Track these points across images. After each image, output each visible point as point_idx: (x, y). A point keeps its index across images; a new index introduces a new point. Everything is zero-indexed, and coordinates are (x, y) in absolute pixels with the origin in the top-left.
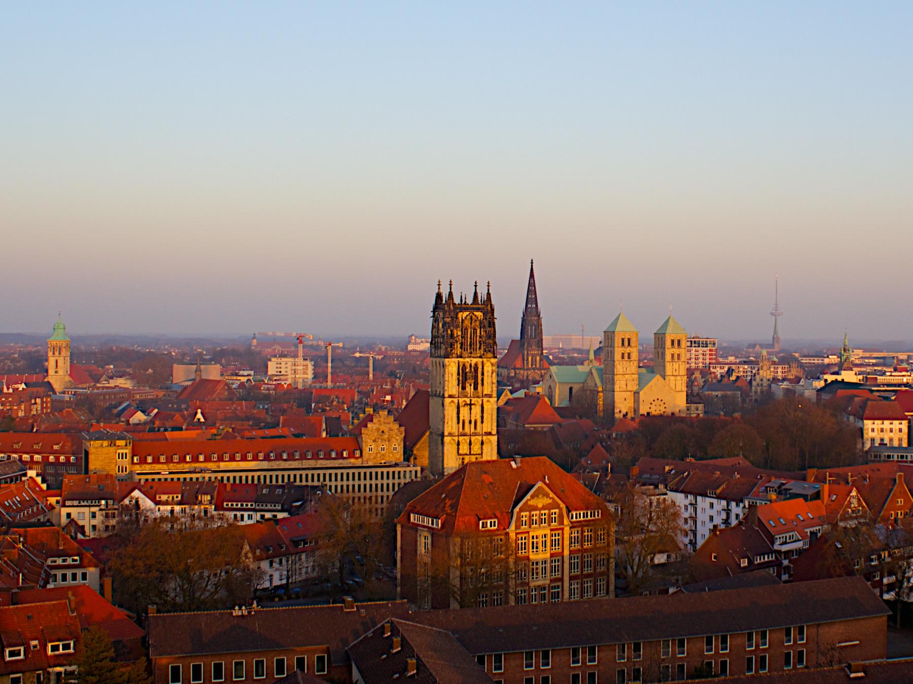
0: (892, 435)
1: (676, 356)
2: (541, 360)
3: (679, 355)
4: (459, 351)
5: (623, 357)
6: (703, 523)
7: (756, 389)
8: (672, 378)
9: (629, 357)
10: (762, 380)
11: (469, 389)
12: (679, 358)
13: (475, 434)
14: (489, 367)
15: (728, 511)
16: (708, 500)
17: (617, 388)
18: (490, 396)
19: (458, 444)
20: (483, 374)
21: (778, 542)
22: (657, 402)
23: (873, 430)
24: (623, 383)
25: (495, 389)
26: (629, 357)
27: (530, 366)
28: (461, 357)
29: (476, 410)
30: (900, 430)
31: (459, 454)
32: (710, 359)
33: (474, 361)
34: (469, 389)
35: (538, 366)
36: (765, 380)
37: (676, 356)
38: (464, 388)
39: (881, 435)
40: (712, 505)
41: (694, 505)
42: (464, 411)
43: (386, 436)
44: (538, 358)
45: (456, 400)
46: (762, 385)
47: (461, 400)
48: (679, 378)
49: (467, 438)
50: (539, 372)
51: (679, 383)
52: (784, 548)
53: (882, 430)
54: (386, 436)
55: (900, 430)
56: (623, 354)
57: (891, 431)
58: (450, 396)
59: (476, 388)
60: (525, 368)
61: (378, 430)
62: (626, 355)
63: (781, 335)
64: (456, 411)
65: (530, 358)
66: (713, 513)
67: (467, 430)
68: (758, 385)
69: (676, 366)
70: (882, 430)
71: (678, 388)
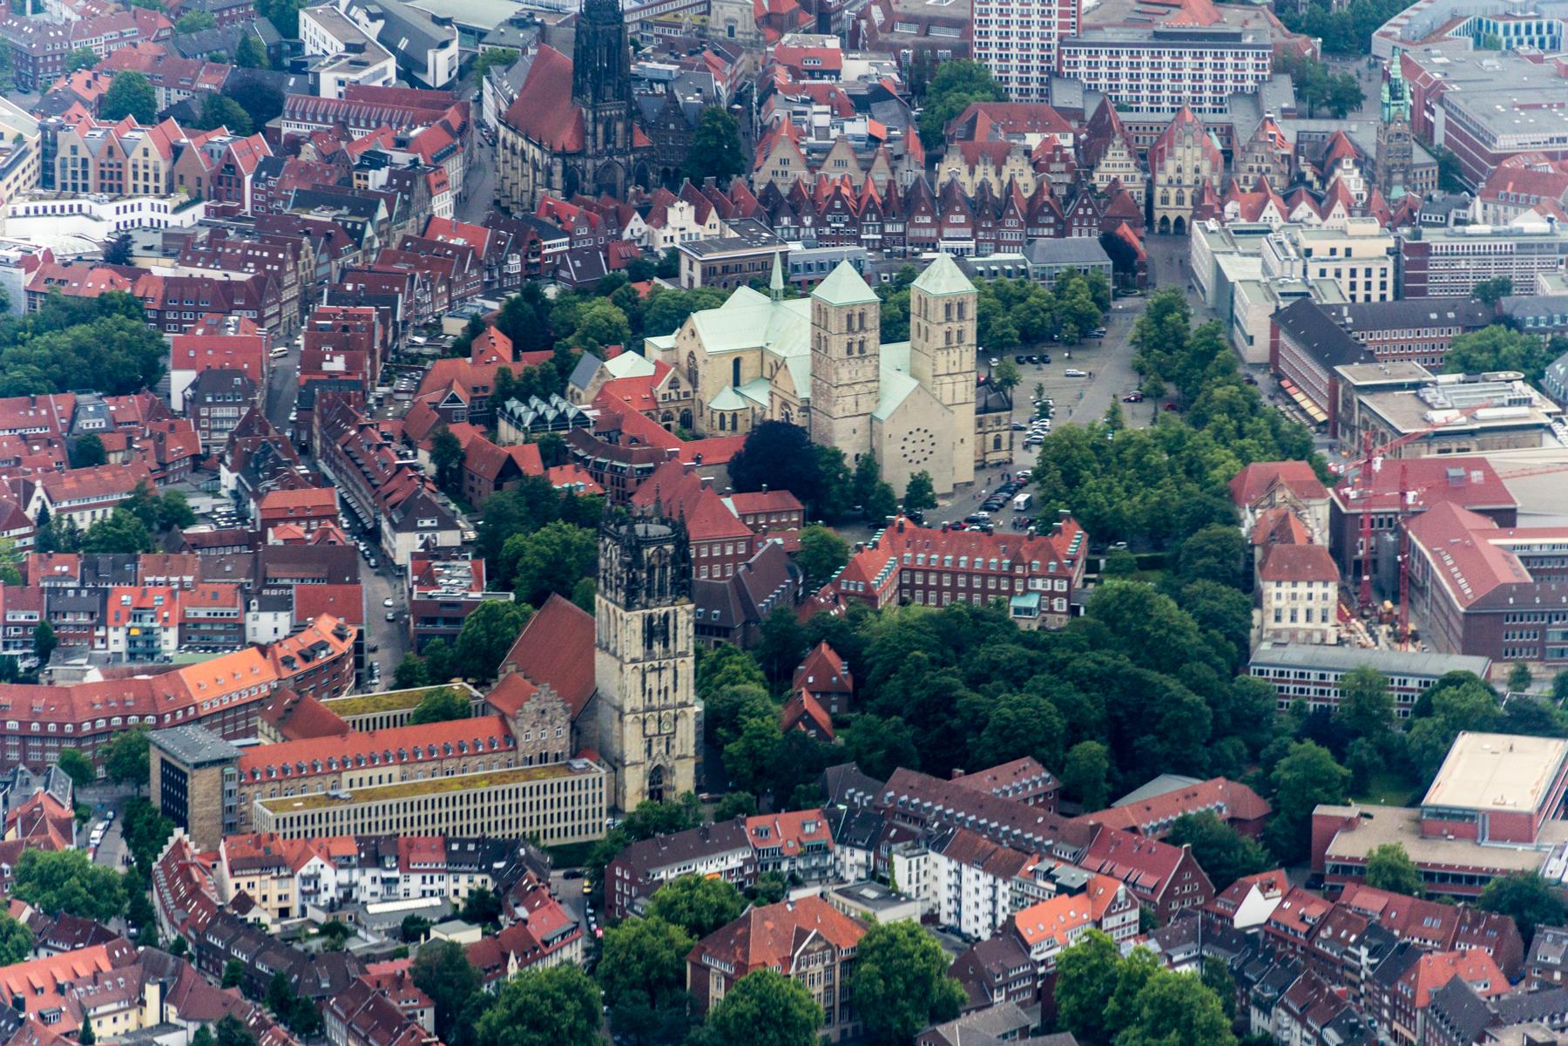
0: (1310, 604)
1: (954, 336)
2: (629, 130)
3: (960, 333)
4: (644, 600)
5: (849, 351)
6: (969, 894)
7: (1165, 190)
8: (947, 379)
9: (861, 350)
10: (1179, 170)
11: (658, 648)
12: (960, 340)
13: (666, 707)
14: (683, 615)
15: (995, 888)
16: (974, 871)
17: (837, 411)
18: (685, 654)
19: (644, 722)
20: (676, 627)
21: (1033, 952)
22: (917, 436)
23: (1279, 596)
24: (850, 400)
25: (692, 645)
26: (861, 350)
27: (600, 147)
28: (646, 607)
29: (668, 675)
30: (1325, 597)
31: (645, 735)
32: (1062, 26)
33: (664, 610)
34: (658, 648)
35: (619, 145)
36: (1188, 171)
37: (954, 336)
38: (650, 647)
39: (1293, 604)
40: (978, 877)
41: (959, 873)
42: (652, 679)
43: (547, 718)
44: (620, 127)
45: (640, 665)
46: (1179, 181)
47: (647, 664)
48: (961, 378)
49: (656, 714)
50: (622, 160)
51: (960, 387)
52: (1040, 958)
53: (1294, 596)
54: (547, 718)
55: (1325, 597)
56: (850, 345)
57: (1310, 597)
58: (634, 661)
59: (666, 645)
60: (590, 152)
61: (537, 711)
62: (856, 347)
63: (1134, 392)
64: (640, 679)
65: (600, 129)
66: (979, 899)
67: (655, 702)
68: (1170, 181)
69: (955, 355)
70: (1294, 596)
71: (960, 398)
